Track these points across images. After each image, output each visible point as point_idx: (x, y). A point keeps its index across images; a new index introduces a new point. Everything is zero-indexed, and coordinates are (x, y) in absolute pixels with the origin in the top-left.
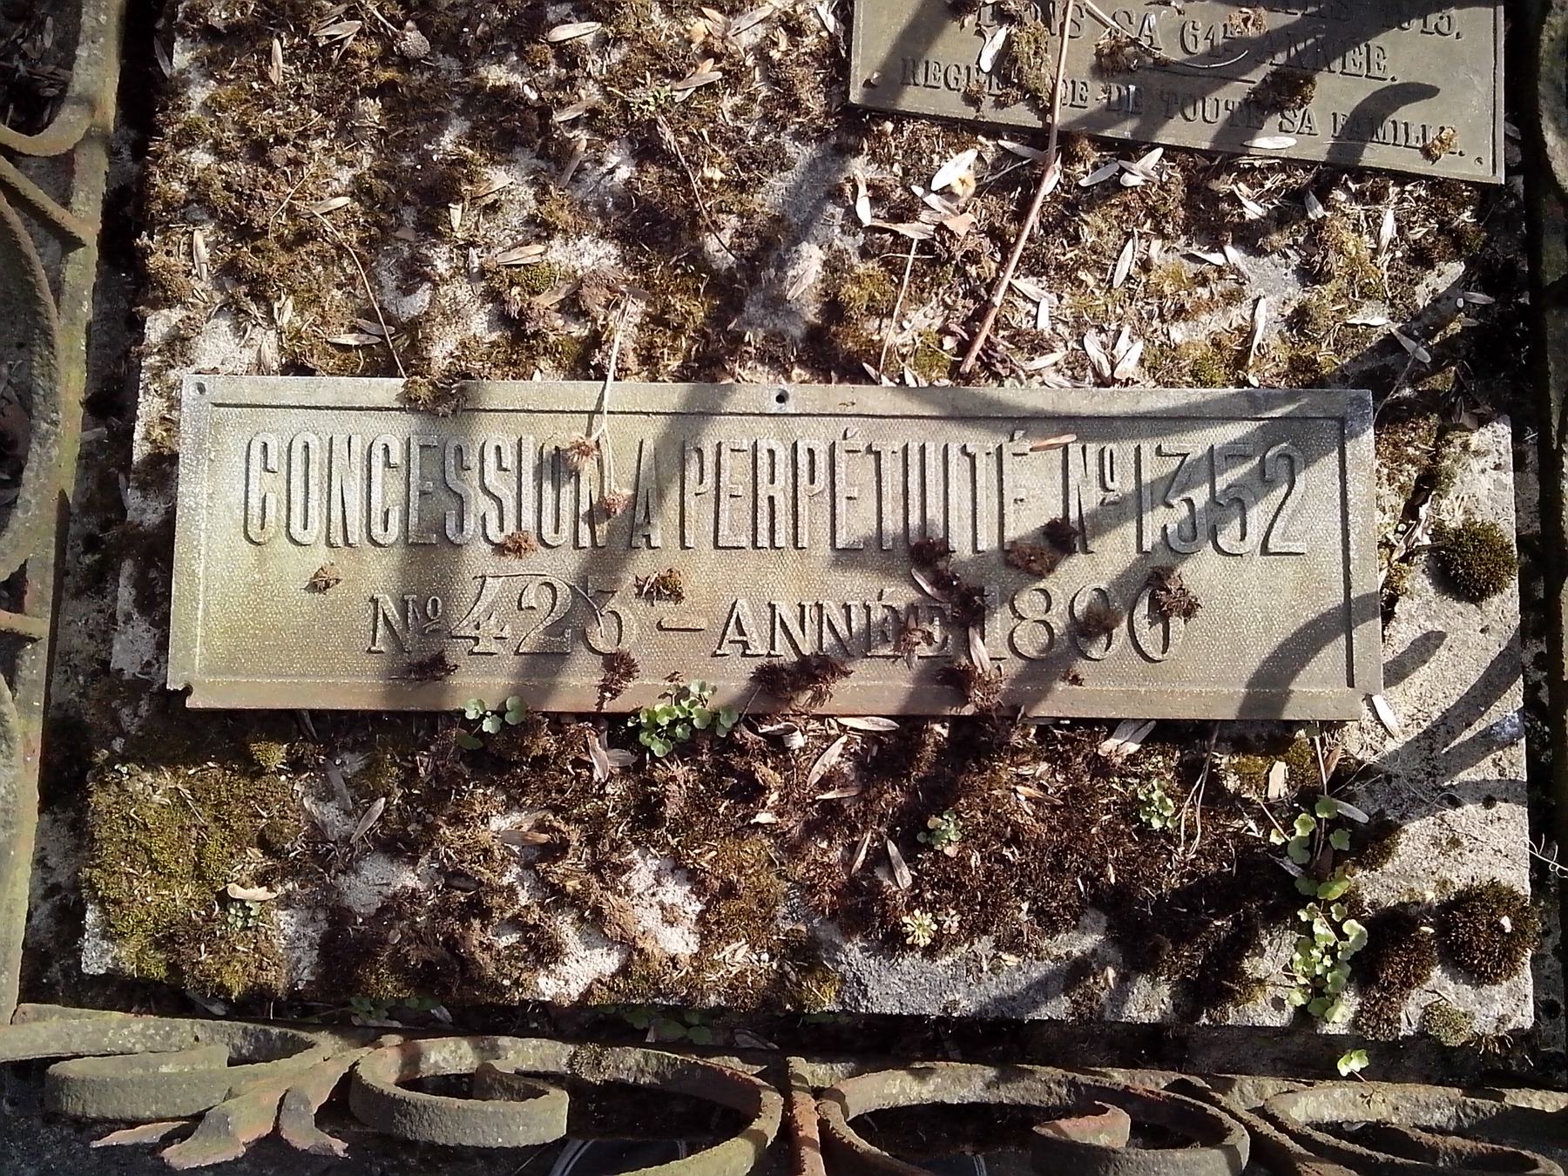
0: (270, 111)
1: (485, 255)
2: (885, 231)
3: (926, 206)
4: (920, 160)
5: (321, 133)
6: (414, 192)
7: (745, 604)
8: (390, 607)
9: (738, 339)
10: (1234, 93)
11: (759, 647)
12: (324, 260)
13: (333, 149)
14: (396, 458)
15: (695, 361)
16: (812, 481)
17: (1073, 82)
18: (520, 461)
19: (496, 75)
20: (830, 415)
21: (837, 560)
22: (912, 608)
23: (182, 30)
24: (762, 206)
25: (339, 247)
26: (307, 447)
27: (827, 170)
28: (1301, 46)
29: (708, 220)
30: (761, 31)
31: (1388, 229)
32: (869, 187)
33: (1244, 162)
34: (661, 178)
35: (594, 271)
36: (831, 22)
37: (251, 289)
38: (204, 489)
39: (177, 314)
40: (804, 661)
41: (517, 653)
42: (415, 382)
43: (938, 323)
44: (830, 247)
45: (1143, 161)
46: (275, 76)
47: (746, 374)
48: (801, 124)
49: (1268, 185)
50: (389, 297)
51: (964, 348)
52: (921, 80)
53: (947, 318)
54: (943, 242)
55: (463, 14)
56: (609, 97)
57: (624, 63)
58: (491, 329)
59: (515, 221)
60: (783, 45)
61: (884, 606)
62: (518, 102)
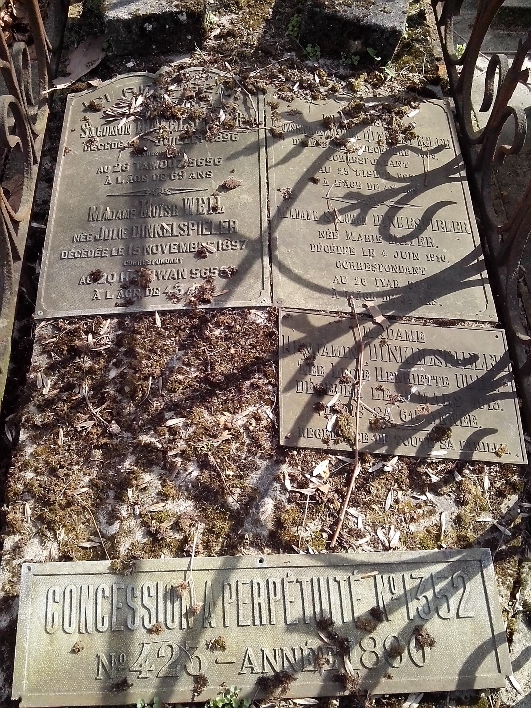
0: (58, 455)
1: (141, 508)
2: (297, 492)
3: (311, 482)
4: (308, 464)
5: (77, 463)
6: (114, 484)
7: (251, 650)
8: (104, 659)
9: (242, 537)
10: (422, 435)
11: (258, 669)
12: (77, 513)
13: (82, 469)
14: (107, 594)
15: (226, 547)
16: (275, 595)
17: (362, 434)
18: (157, 593)
19: (145, 439)
20: (280, 567)
21: (288, 629)
22: (320, 649)
23: (24, 426)
24: (249, 484)
25: (84, 508)
26: (71, 591)
27: (273, 470)
28: (444, 417)
29: (228, 491)
30: (245, 419)
31: (487, 484)
32: (289, 476)
33: (429, 460)
34: (210, 475)
35: (185, 513)
36: (271, 416)
37: (48, 526)
38: (30, 610)
39: (17, 537)
40: (277, 674)
41: (157, 677)
42: (115, 562)
43: (320, 527)
44: (276, 499)
45: (391, 461)
46: (60, 442)
47: (246, 551)
48: (262, 453)
49: (439, 468)
50: (103, 526)
51: (331, 537)
52: (306, 435)
53: (323, 525)
54: (319, 496)
55: (133, 417)
56: (189, 446)
57: (194, 433)
58: (144, 538)
59: (153, 494)
60: (254, 424)
61: (308, 648)
62: (154, 449)
